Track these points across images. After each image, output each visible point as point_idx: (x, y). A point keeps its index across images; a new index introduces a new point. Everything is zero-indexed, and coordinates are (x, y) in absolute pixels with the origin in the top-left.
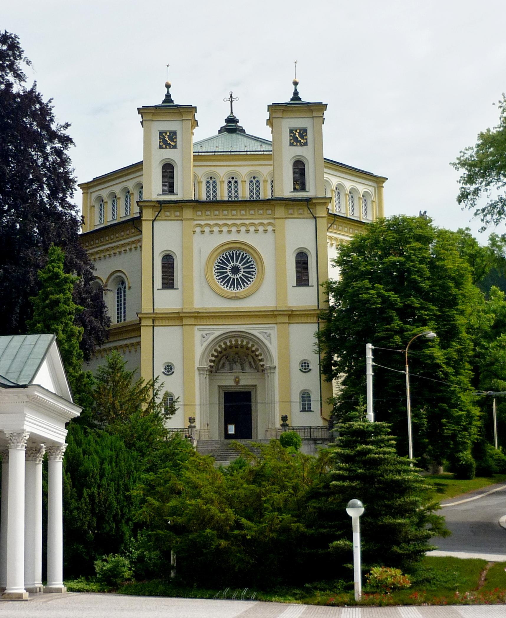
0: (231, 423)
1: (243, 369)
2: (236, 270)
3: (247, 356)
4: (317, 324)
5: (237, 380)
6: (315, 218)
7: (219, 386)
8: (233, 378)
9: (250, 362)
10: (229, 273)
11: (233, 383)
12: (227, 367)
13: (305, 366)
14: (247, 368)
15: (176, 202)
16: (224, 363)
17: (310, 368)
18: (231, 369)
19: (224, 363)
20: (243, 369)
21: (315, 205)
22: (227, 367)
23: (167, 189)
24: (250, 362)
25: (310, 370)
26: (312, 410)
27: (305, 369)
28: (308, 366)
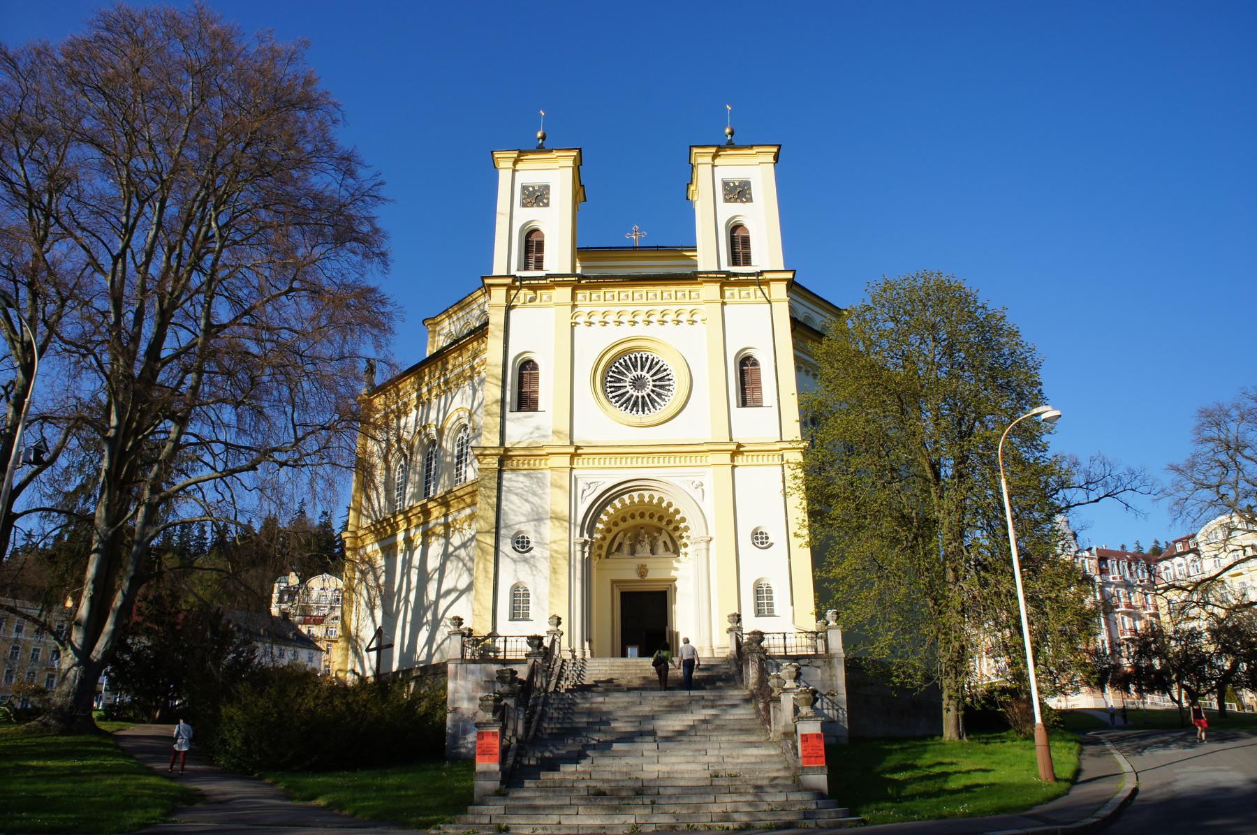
0: (632, 644)
1: (653, 552)
2: (638, 383)
3: (659, 530)
4: (780, 468)
5: (642, 571)
6: (769, 302)
7: (613, 582)
8: (636, 567)
9: (665, 543)
10: (629, 388)
11: (635, 576)
12: (626, 549)
13: (762, 538)
14: (661, 549)
15: (548, 276)
16: (620, 544)
17: (770, 541)
18: (633, 552)
19: (620, 544)
20: (653, 552)
21: (767, 283)
22: (626, 549)
23: (532, 265)
24: (665, 543)
25: (771, 544)
26: (776, 613)
27: (762, 543)
28: (767, 538)
